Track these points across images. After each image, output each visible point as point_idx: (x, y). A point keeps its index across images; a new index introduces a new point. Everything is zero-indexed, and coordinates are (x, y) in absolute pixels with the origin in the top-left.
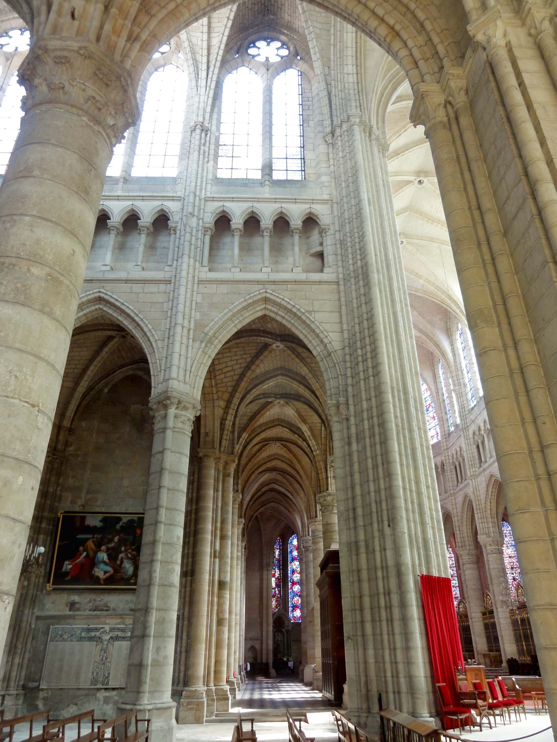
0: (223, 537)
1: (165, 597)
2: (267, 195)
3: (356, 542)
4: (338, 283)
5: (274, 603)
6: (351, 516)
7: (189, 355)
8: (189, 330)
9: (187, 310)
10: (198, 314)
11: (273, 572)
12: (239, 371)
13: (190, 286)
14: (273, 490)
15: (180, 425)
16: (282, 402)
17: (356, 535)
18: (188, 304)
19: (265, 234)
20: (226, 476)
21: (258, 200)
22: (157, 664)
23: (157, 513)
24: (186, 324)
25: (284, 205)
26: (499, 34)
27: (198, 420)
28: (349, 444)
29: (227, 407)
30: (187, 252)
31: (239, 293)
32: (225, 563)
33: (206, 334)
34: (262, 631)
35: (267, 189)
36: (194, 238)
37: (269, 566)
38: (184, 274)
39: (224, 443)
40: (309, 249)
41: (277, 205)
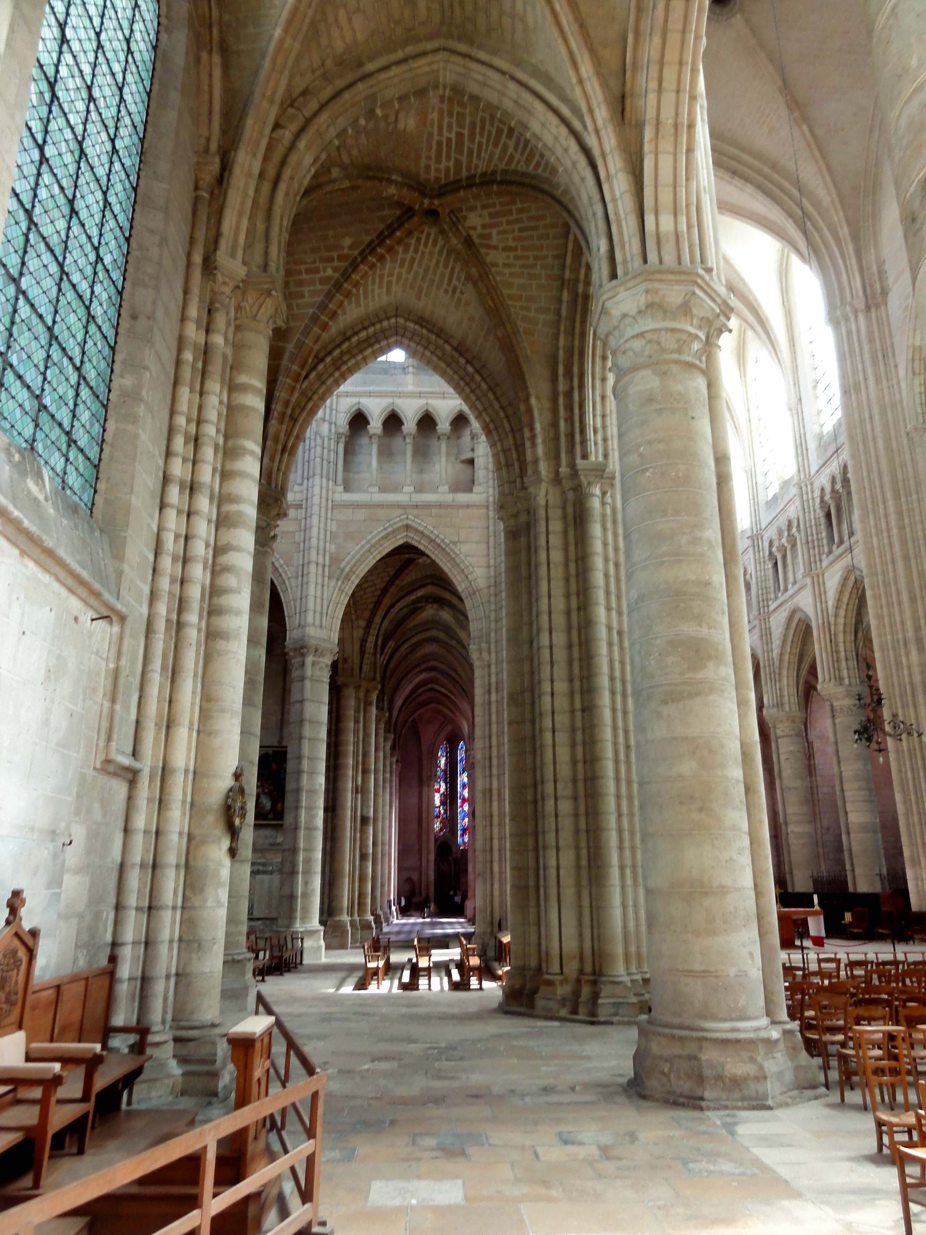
0: (365, 771)
1: (310, 839)
2: (410, 388)
3: (491, 790)
4: (487, 507)
5: (437, 826)
6: (487, 764)
7: (325, 596)
8: (324, 566)
9: (321, 543)
10: (333, 546)
11: (436, 787)
12: (382, 585)
13: (323, 514)
14: (432, 690)
15: (318, 673)
16: (435, 606)
17: (491, 784)
18: (322, 536)
19: (408, 440)
20: (368, 704)
21: (401, 395)
22: (305, 895)
23: (300, 763)
24: (321, 560)
25: (431, 401)
26: (542, 493)
27: (335, 666)
28: (489, 692)
29: (368, 627)
30: (318, 471)
31: (378, 520)
32: (368, 799)
33: (343, 570)
34: (421, 859)
35: (410, 378)
36: (326, 451)
37: (433, 778)
38: (316, 500)
39: (366, 668)
40: (459, 453)
41: (422, 402)
